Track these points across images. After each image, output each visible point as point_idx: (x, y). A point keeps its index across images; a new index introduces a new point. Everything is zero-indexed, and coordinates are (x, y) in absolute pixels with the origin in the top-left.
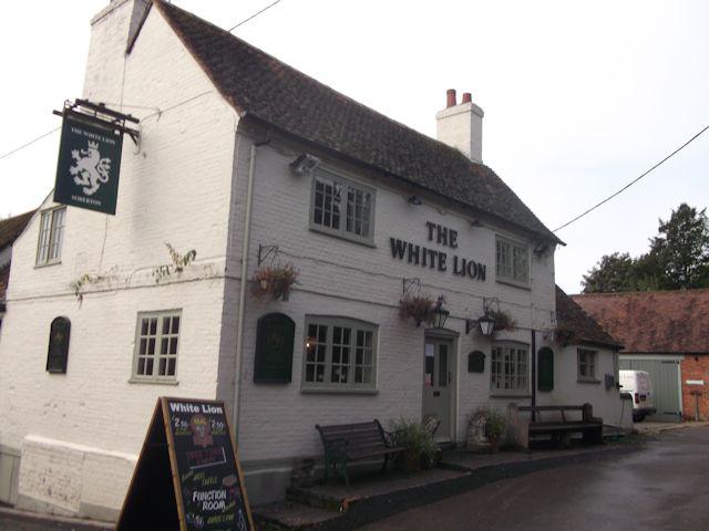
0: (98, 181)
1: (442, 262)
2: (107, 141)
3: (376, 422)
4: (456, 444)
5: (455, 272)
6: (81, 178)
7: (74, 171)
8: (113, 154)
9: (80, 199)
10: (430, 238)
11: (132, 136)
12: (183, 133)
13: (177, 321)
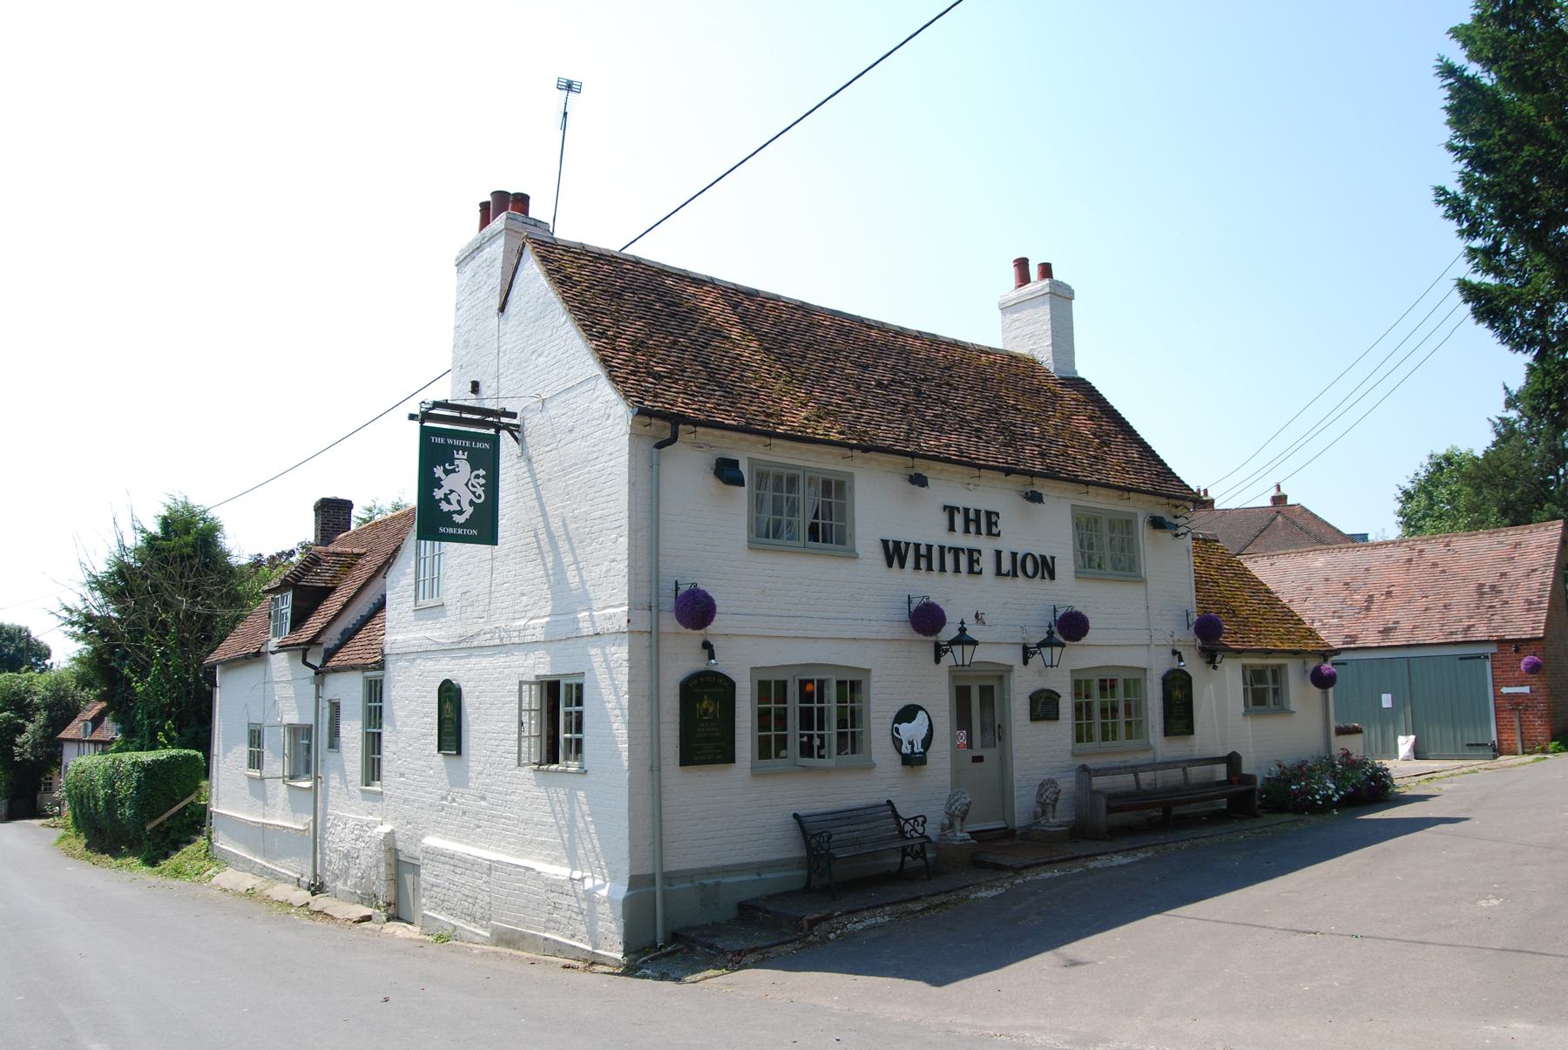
0: (471, 503)
1: (972, 562)
2: (479, 445)
3: (889, 803)
4: (1014, 831)
5: (999, 573)
6: (449, 502)
7: (438, 494)
8: (487, 461)
9: (450, 530)
10: (952, 528)
11: (511, 432)
12: (571, 431)
13: (580, 687)
